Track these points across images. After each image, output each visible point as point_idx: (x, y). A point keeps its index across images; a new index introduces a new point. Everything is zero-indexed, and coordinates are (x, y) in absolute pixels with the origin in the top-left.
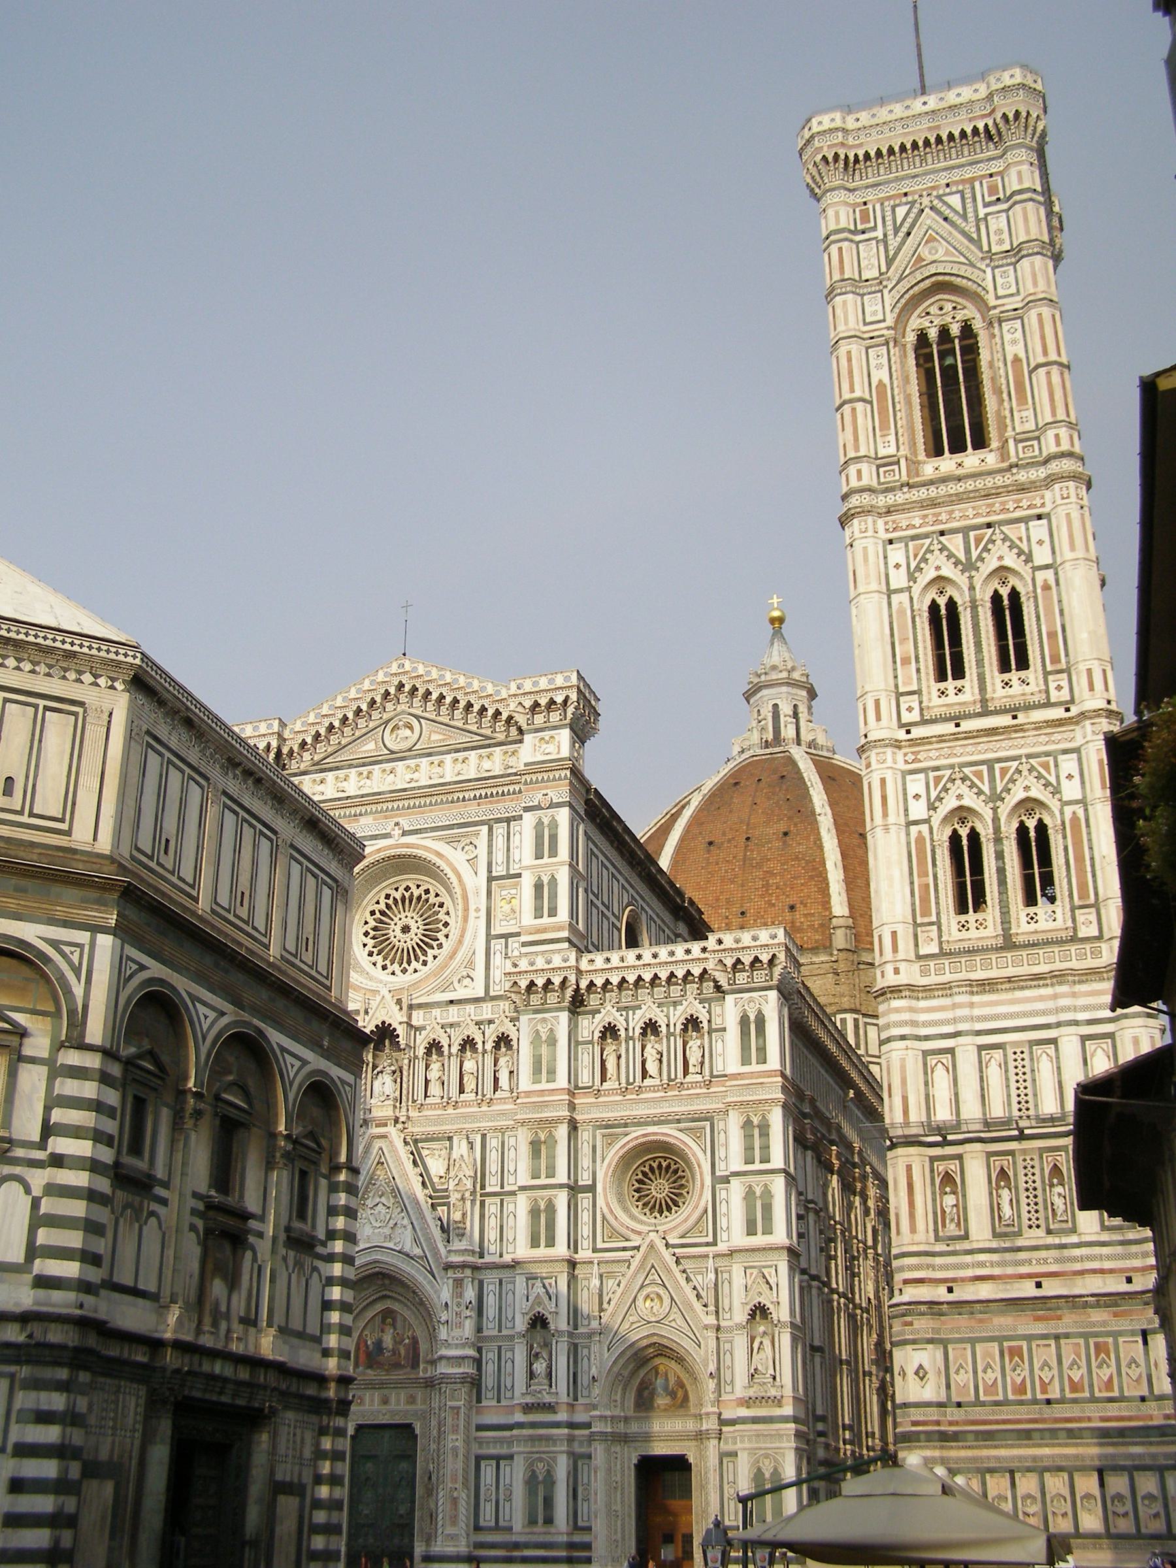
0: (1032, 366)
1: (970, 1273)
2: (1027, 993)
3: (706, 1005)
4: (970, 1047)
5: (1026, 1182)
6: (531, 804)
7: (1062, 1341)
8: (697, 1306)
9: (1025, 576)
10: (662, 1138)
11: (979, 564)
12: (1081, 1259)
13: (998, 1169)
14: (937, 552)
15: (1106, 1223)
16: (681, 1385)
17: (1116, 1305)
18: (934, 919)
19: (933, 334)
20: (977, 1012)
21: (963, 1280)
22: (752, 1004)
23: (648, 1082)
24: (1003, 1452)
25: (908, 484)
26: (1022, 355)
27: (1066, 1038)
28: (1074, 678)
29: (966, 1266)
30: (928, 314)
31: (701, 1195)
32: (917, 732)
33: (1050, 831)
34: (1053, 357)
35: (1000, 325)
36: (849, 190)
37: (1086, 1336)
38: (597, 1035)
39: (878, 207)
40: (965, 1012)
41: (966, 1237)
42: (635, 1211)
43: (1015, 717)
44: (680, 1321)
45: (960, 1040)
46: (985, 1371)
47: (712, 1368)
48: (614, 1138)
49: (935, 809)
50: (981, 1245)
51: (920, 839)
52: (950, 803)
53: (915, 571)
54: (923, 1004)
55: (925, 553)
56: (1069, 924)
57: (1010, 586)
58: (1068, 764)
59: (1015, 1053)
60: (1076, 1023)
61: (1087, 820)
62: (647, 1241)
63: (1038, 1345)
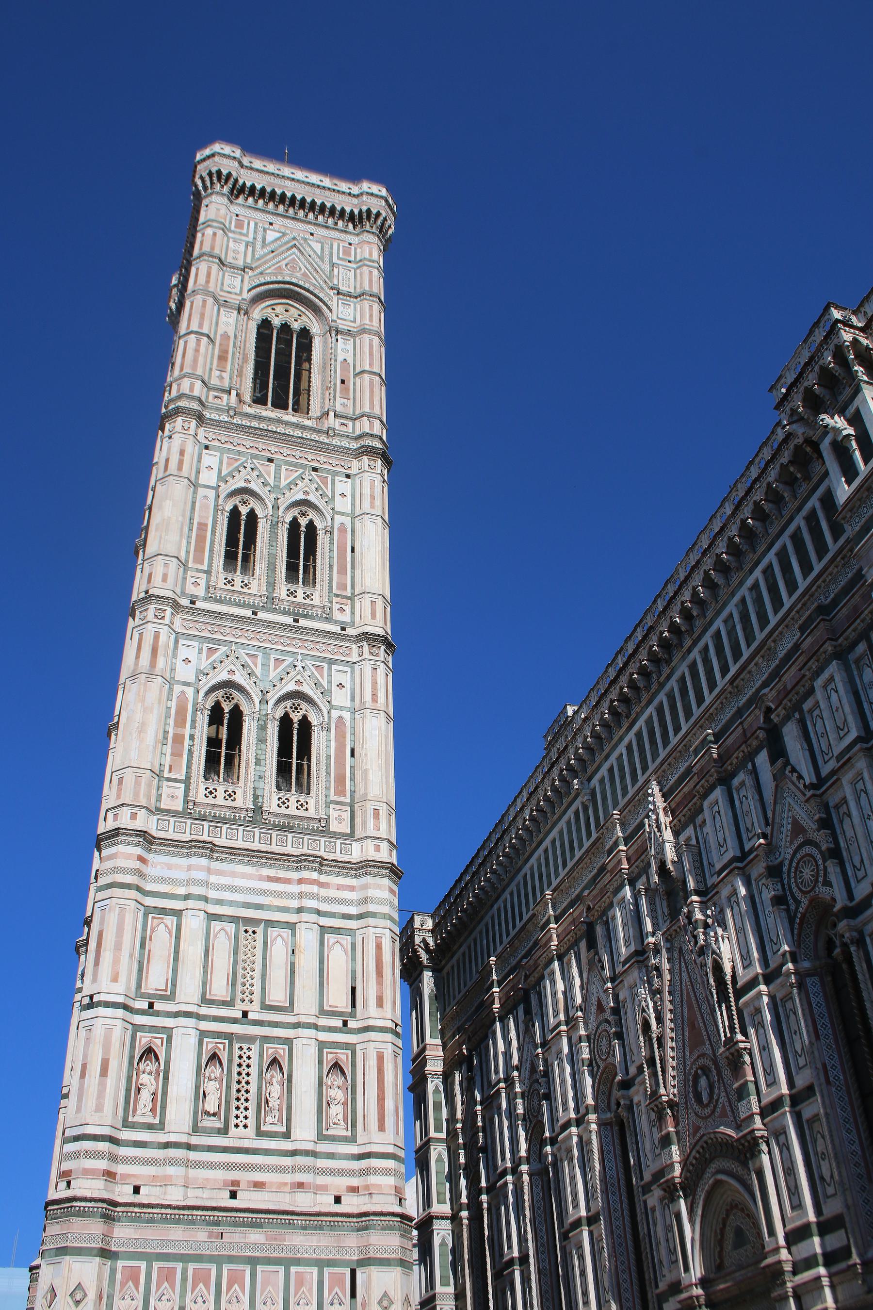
0: (358, 370)
7: (260, 1268)
9: (325, 513)
11: (286, 491)
12: (294, 1169)
14: (249, 469)
19: (276, 322)
20: (213, 879)
25: (235, 409)
26: (350, 360)
30: (273, 309)
32: (199, 604)
34: (376, 369)
35: (336, 335)
36: (231, 202)
39: (252, 224)
40: (201, 875)
41: (161, 1126)
43: (296, 621)
53: (226, 476)
55: (239, 466)
57: (308, 518)
59: (246, 931)
61: (353, 728)
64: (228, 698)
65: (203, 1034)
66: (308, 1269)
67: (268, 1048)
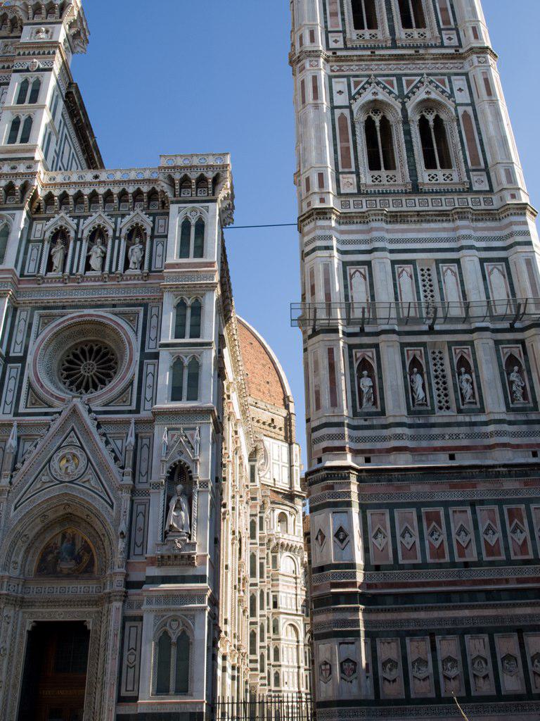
2: (433, 225)
3: (151, 218)
5: (436, 371)
6: (21, 68)
8: (114, 467)
10: (97, 319)
13: (411, 358)
15: (511, 406)
16: (87, 549)
17: (526, 475)
18: (353, 169)
21: (380, 451)
22: (193, 213)
23: (88, 273)
24: (422, 615)
27: (468, 258)
28: (461, 34)
29: (384, 439)
31: (128, 369)
32: (339, 53)
33: (445, 123)
37: (500, 503)
38: (48, 235)
41: (383, 413)
42: (61, 386)
44: (93, 483)
45: (376, 254)
46: (403, 536)
47: (123, 527)
48: (53, 317)
49: (355, 99)
50: (398, 420)
51: (342, 118)
52: (367, 96)
56: (466, 179)
58: (459, 82)
59: (422, 270)
60: (478, 249)
62: (71, 406)
63: (454, 512)
64: (376, 113)
65: (403, 345)
66: (519, 506)
67: (455, 349)
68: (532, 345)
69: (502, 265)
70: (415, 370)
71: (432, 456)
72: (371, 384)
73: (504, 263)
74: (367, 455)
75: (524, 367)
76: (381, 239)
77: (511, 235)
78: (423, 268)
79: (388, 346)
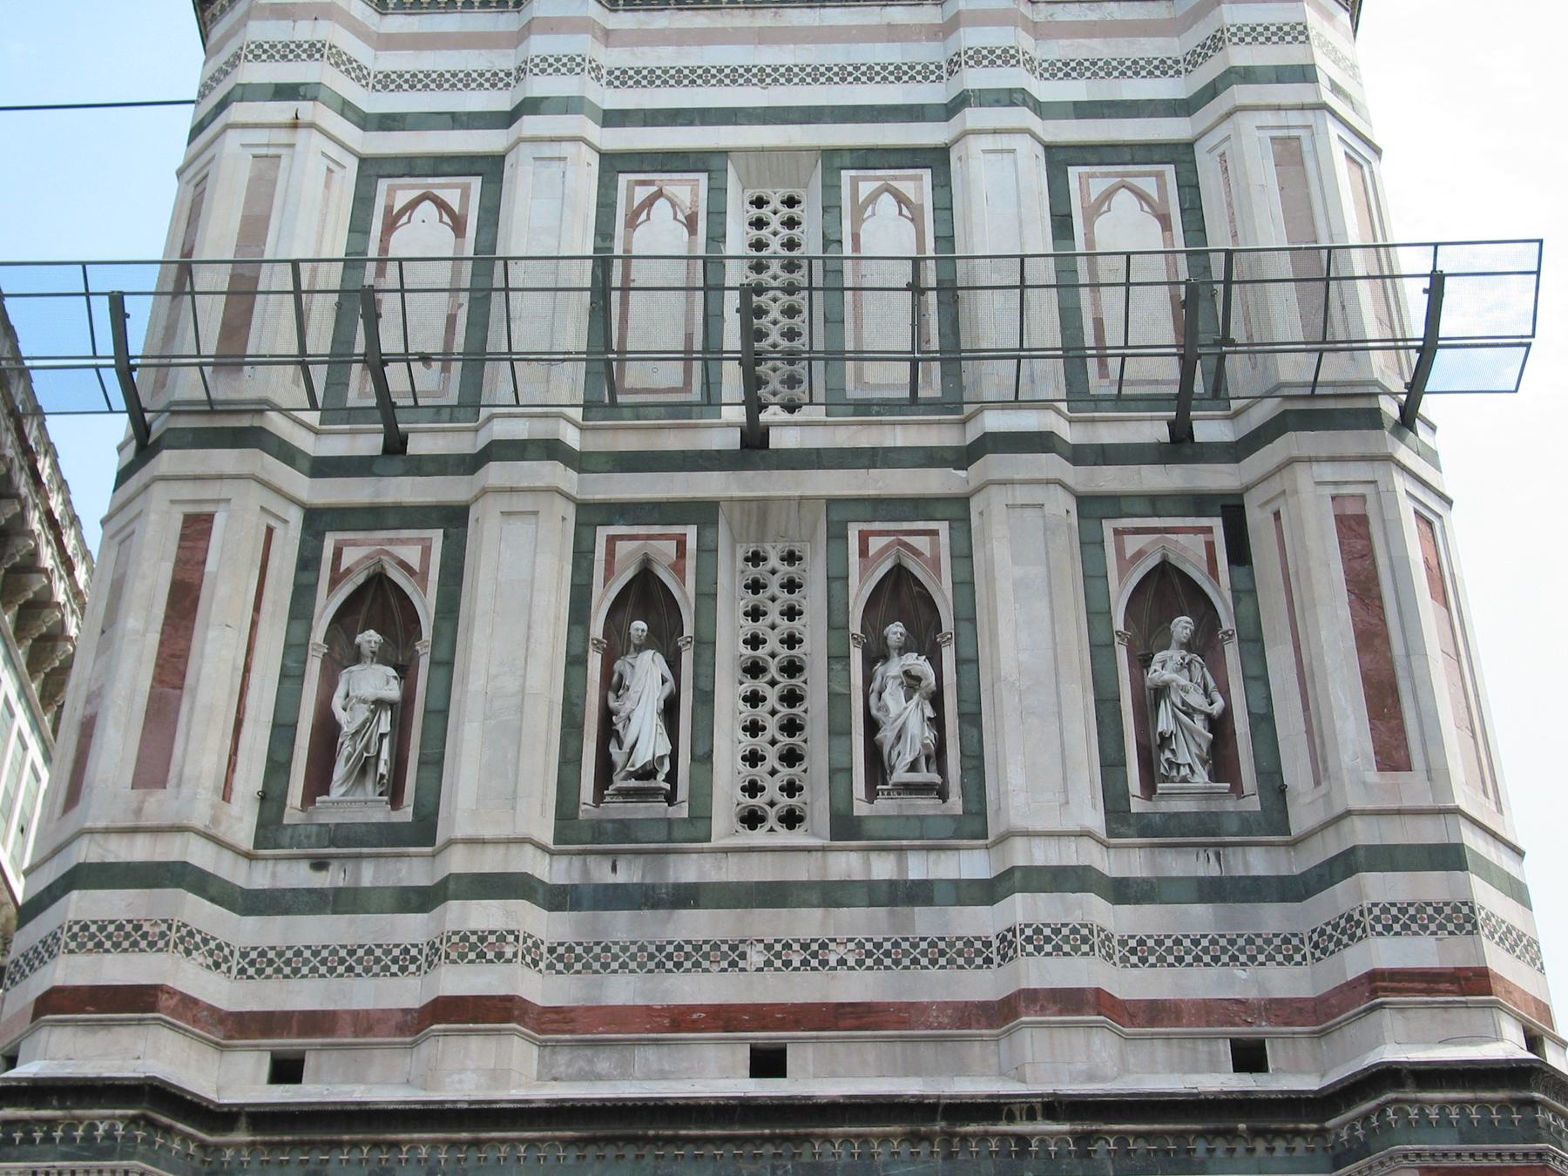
1: (409, 993)
4: (567, 149)
12: (1006, 946)
15: (1137, 806)
21: (366, 1023)
27: (988, 142)
29: (404, 960)
50: (490, 862)
54: (397, 24)
59: (759, 202)
65: (591, 514)
67: (864, 537)
68: (1277, 515)
69: (1159, 176)
70: (639, 626)
71: (651, 1053)
72: (393, 692)
73: (1169, 171)
74: (288, 1043)
75: (1227, 623)
76: (572, 65)
77: (1216, 42)
78: (766, 192)
79: (506, 514)
